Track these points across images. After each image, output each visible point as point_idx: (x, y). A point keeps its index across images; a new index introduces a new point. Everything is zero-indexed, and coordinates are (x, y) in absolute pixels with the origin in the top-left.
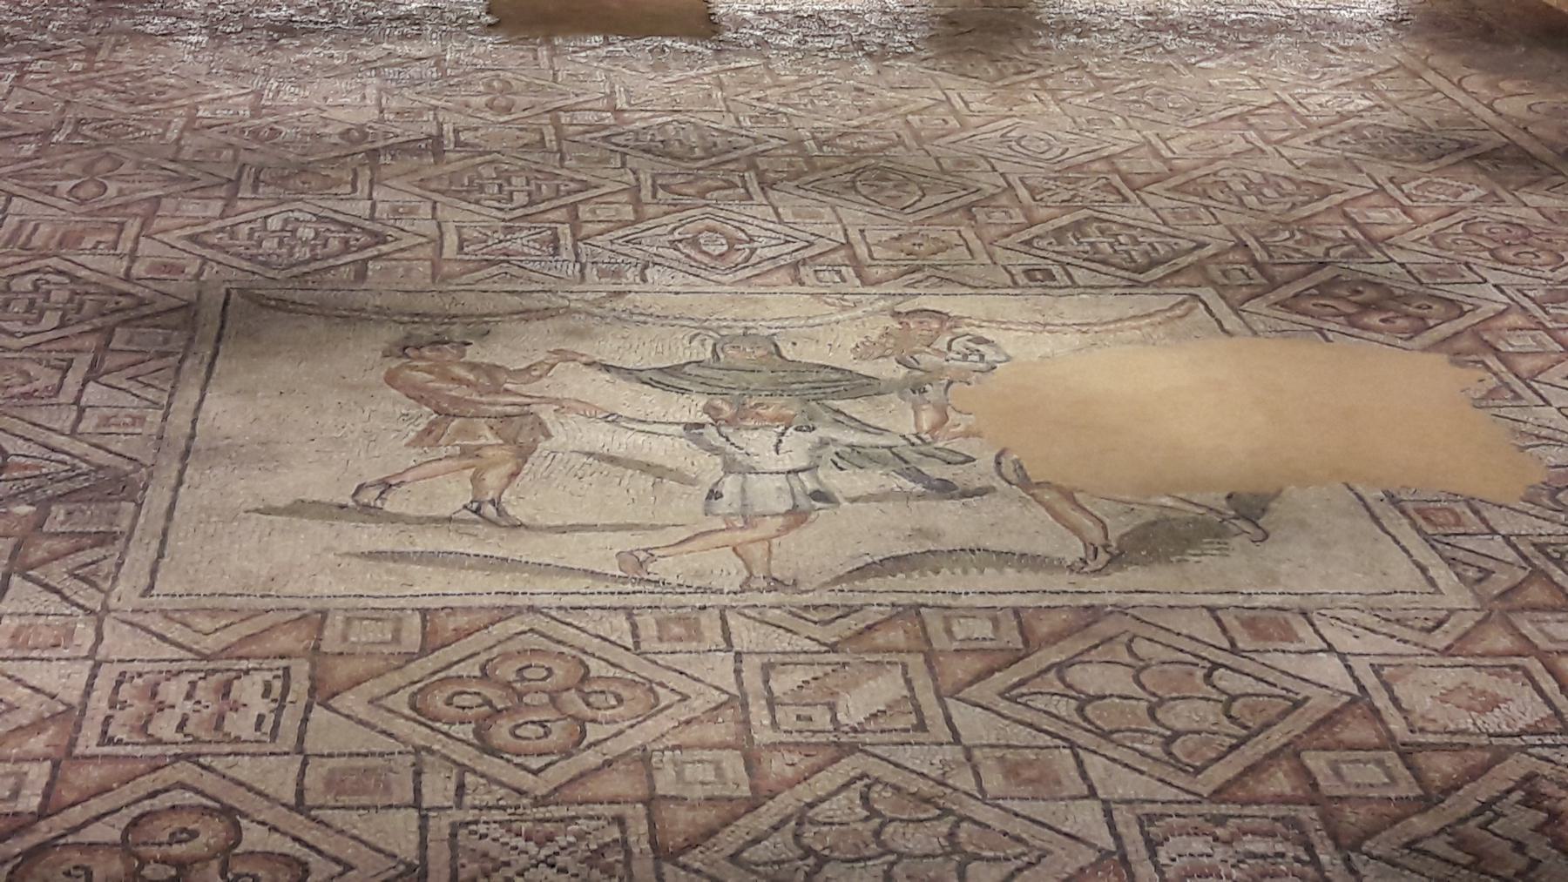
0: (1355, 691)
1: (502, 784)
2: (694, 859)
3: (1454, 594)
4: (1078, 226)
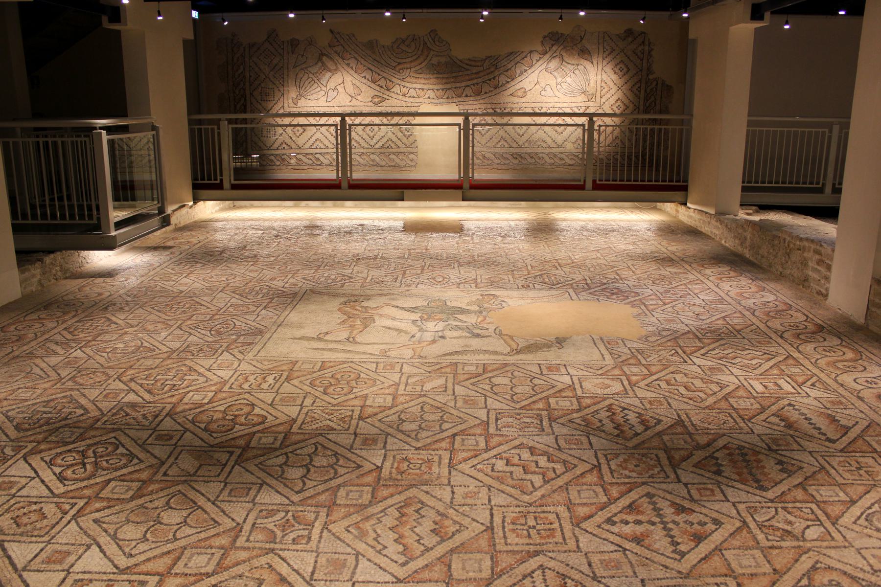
0: (571, 383)
1: (325, 401)
2: (368, 420)
3: (609, 361)
4: (541, 275)
